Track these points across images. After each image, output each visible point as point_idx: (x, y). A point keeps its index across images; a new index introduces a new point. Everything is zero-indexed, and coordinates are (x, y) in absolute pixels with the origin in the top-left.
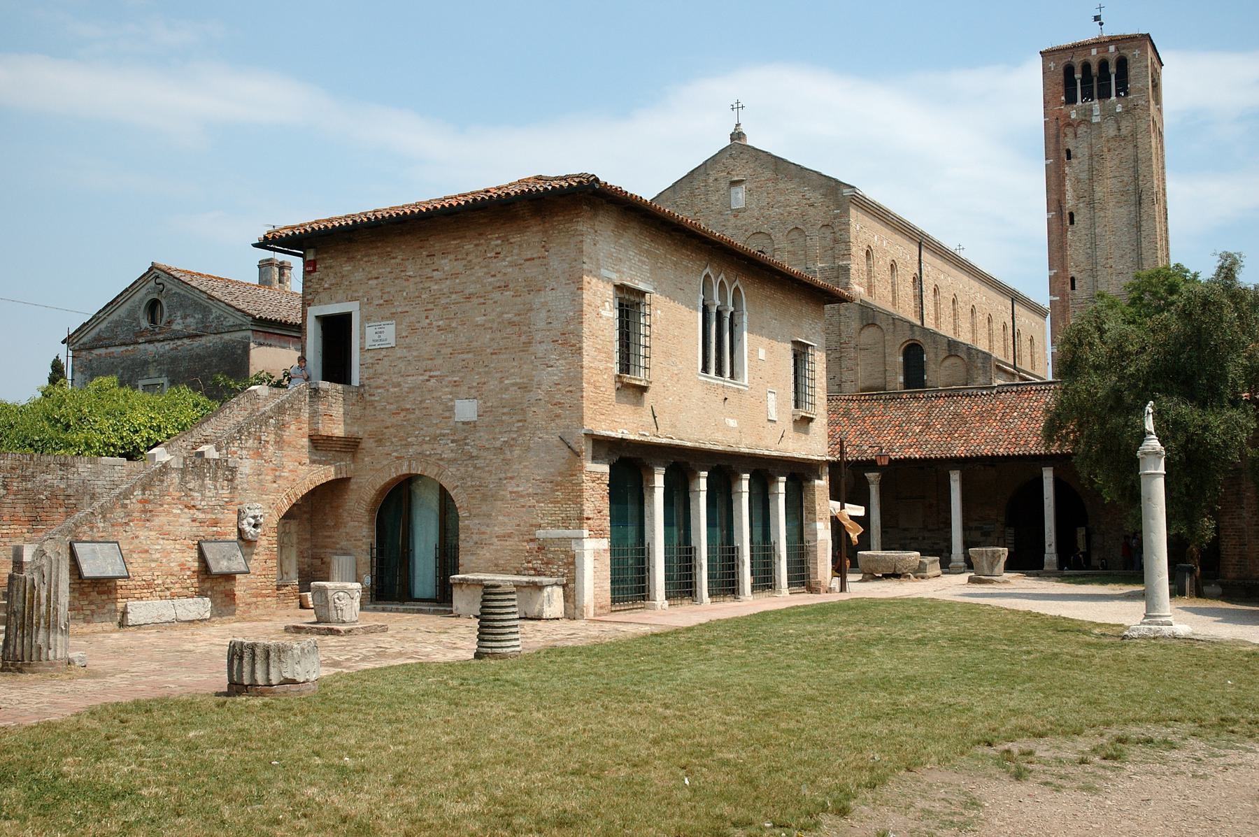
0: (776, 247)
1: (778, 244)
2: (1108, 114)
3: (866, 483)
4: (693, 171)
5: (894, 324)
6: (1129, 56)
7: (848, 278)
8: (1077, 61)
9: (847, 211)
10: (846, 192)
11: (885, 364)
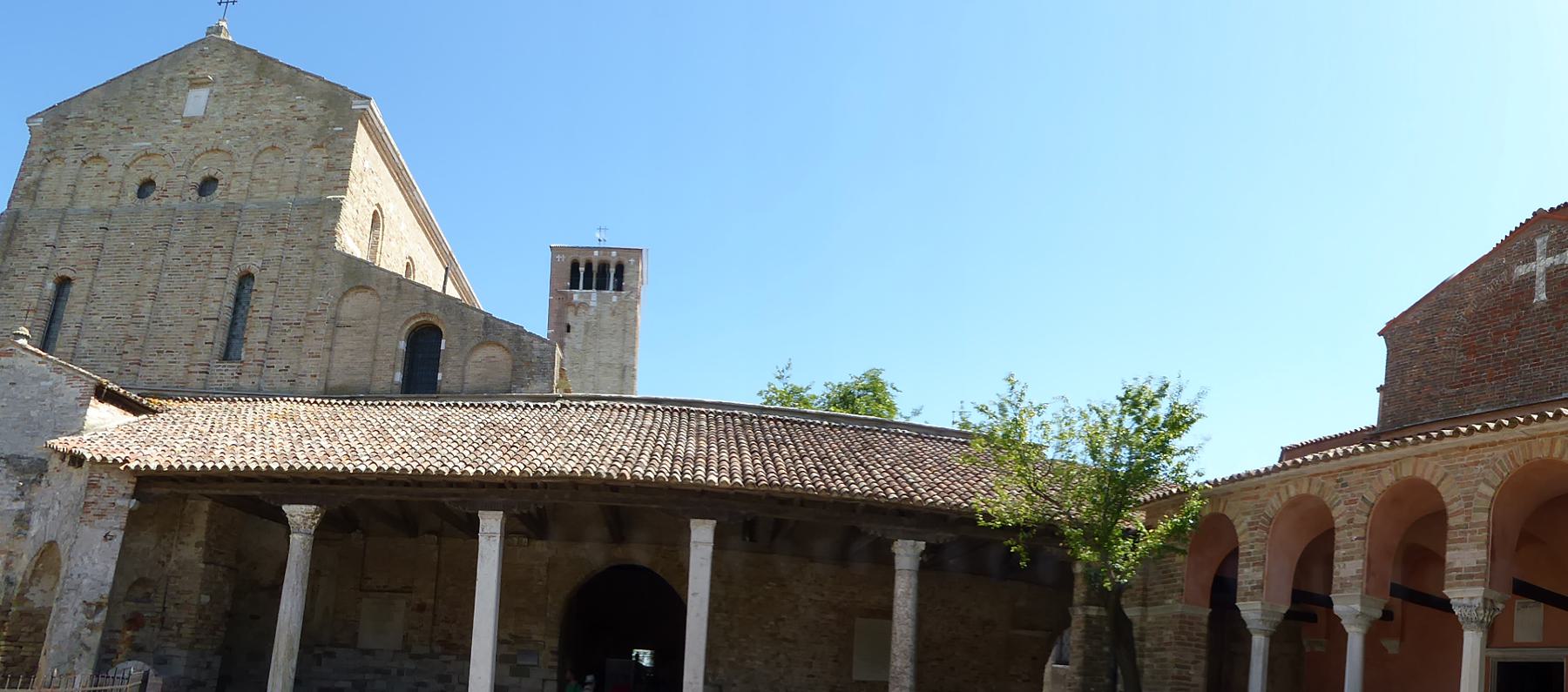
0: (236, 170)
1: (239, 166)
4: (142, 66)
5: (399, 288)
10: (357, 105)
11: (375, 349)
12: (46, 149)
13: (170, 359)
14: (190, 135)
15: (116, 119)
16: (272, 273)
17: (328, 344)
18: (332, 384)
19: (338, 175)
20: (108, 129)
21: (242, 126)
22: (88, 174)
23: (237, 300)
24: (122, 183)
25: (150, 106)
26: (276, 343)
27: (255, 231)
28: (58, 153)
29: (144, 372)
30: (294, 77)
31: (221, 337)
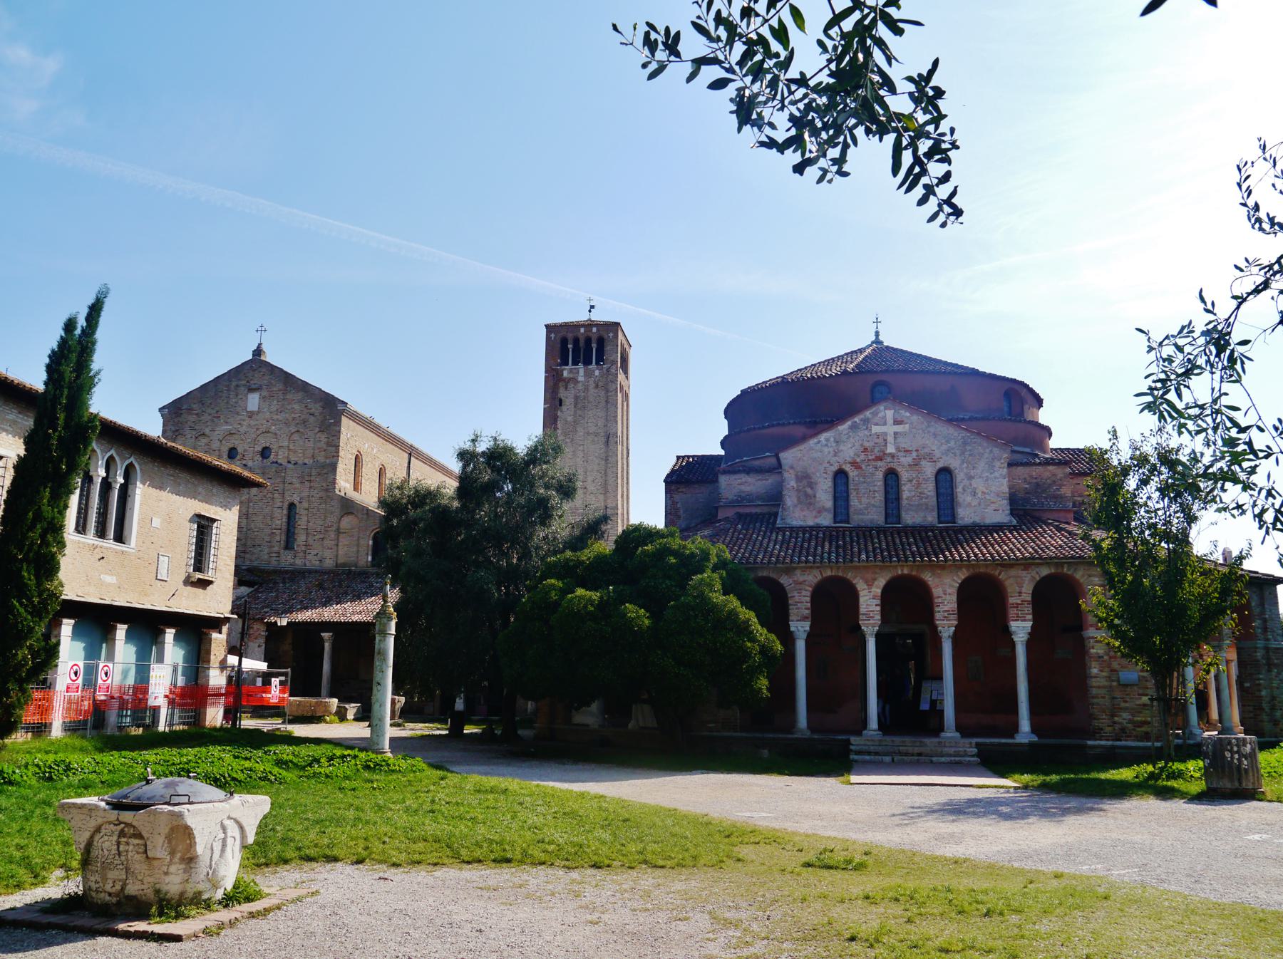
0: (281, 444)
2: (589, 374)
3: (322, 641)
4: (218, 377)
6: (606, 337)
7: (335, 475)
8: (570, 336)
9: (338, 423)
10: (340, 407)
11: (358, 545)
12: (173, 429)
13: (259, 549)
14: (253, 423)
15: (209, 411)
16: (305, 505)
17: (335, 542)
18: (339, 562)
19: (333, 449)
20: (206, 417)
21: (281, 419)
22: (200, 444)
23: (289, 517)
24: (219, 450)
25: (227, 403)
26: (310, 541)
27: (294, 480)
28: (181, 431)
29: (247, 556)
30: (304, 387)
31: (284, 537)
